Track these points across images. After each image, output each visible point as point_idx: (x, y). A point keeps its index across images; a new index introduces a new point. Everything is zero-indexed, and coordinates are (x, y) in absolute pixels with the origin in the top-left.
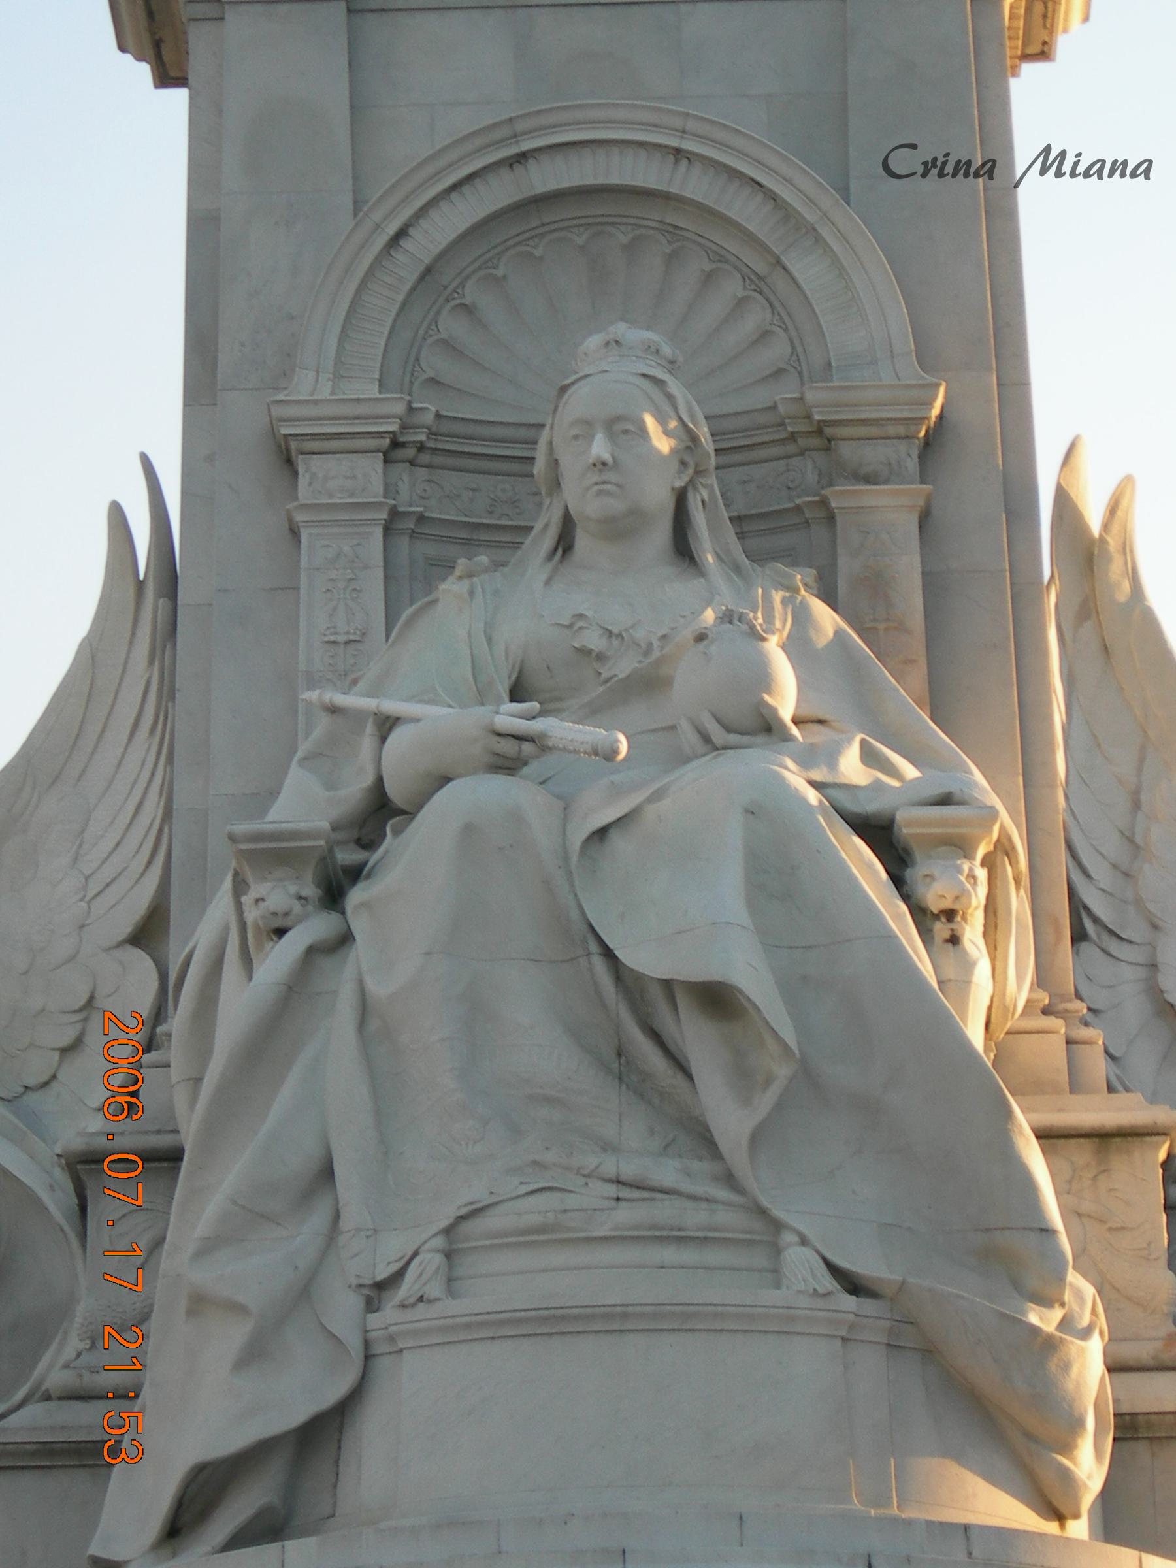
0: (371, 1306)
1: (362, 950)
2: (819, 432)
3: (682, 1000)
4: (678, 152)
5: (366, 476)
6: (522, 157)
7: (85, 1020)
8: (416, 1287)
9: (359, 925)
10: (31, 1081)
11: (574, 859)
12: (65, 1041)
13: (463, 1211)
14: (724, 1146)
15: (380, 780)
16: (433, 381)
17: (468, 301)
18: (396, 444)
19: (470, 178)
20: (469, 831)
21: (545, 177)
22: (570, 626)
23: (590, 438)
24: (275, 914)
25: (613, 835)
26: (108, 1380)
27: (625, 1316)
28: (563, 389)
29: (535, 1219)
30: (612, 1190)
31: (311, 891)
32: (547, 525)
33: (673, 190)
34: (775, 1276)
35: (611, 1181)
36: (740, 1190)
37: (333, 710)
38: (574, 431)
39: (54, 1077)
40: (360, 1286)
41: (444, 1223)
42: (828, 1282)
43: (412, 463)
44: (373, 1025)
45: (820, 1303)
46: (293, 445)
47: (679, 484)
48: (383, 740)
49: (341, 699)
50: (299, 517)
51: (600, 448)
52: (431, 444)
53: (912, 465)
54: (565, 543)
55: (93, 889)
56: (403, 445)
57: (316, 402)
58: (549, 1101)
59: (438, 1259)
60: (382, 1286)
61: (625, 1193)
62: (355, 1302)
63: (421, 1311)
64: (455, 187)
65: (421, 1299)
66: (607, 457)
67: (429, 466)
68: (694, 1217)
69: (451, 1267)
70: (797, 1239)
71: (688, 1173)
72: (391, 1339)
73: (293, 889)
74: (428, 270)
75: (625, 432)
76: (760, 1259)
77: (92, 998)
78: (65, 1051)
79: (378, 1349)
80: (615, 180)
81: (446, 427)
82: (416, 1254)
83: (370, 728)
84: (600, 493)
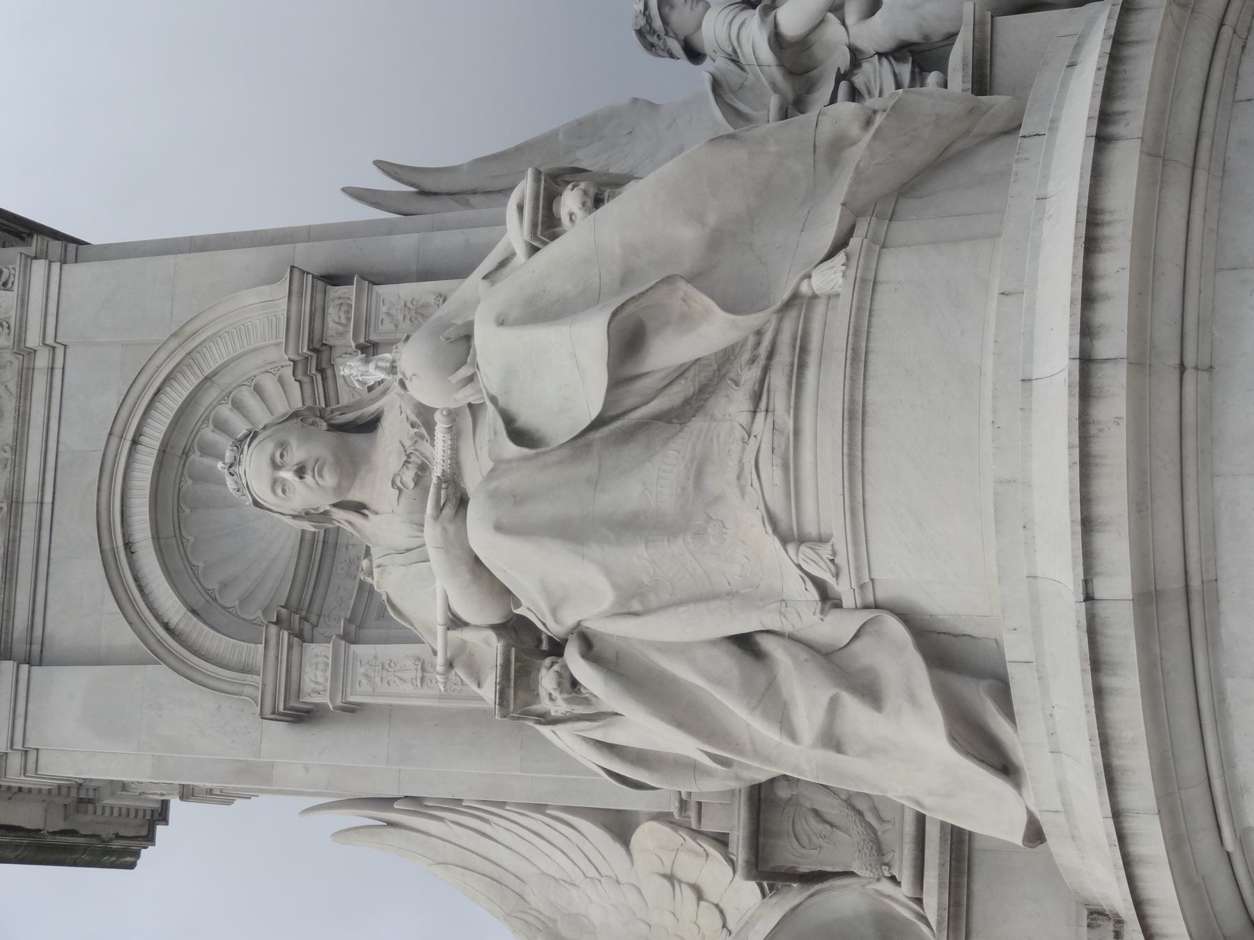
0: (838, 605)
4: (135, 442)
5: (318, 655)
6: (128, 545)
7: (680, 882)
8: (822, 564)
9: (569, 618)
10: (720, 923)
13: (769, 529)
15: (494, 627)
16: (265, 611)
17: (216, 587)
18: (300, 636)
19: (136, 579)
20: (499, 528)
22: (400, 490)
23: (284, 481)
24: (559, 684)
28: (256, 503)
29: (778, 474)
30: (760, 416)
31: (548, 661)
32: (350, 523)
33: (157, 445)
34: (833, 297)
35: (753, 418)
37: (450, 665)
38: (279, 491)
39: (717, 906)
40: (823, 612)
41: (778, 544)
42: (840, 257)
43: (314, 626)
44: (636, 606)
45: (854, 263)
46: (293, 704)
47: (324, 425)
48: (466, 624)
50: (339, 702)
52: (304, 613)
54: (359, 508)
55: (592, 872)
56: (301, 631)
57: (264, 685)
58: (699, 475)
59: (803, 548)
61: (763, 405)
62: (834, 615)
63: (841, 560)
67: (319, 616)
68: (784, 355)
69: (811, 540)
70: (806, 281)
71: (753, 361)
72: (862, 587)
73: (543, 672)
74: (194, 612)
75: (282, 456)
76: (820, 308)
77: (664, 876)
78: (700, 895)
79: (870, 599)
81: (294, 602)
82: (799, 567)
83: (456, 635)
84: (321, 475)
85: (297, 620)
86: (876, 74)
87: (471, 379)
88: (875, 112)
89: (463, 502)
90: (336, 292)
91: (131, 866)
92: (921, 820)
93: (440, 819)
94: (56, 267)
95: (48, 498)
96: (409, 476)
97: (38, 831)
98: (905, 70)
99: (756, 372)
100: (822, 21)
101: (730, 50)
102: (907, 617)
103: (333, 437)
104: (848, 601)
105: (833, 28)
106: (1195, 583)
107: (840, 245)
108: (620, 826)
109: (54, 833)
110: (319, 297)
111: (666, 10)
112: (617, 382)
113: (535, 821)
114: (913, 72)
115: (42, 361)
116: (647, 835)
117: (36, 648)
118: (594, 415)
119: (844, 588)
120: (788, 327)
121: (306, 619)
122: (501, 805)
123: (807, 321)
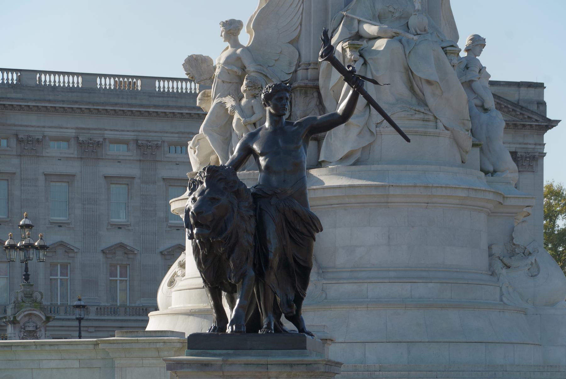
9: (369, 61)
10: (270, 65)
15: (358, 31)
30: (414, 112)
36: (431, 112)
42: (444, 129)
62: (375, 126)
68: (426, 117)
83: (356, 22)
99: (423, 111)
104: (378, 129)
106: (389, 204)
107: (447, 129)
108: (294, 42)
112: (420, 78)
116: (292, 48)
120: (432, 118)
122: (302, 14)
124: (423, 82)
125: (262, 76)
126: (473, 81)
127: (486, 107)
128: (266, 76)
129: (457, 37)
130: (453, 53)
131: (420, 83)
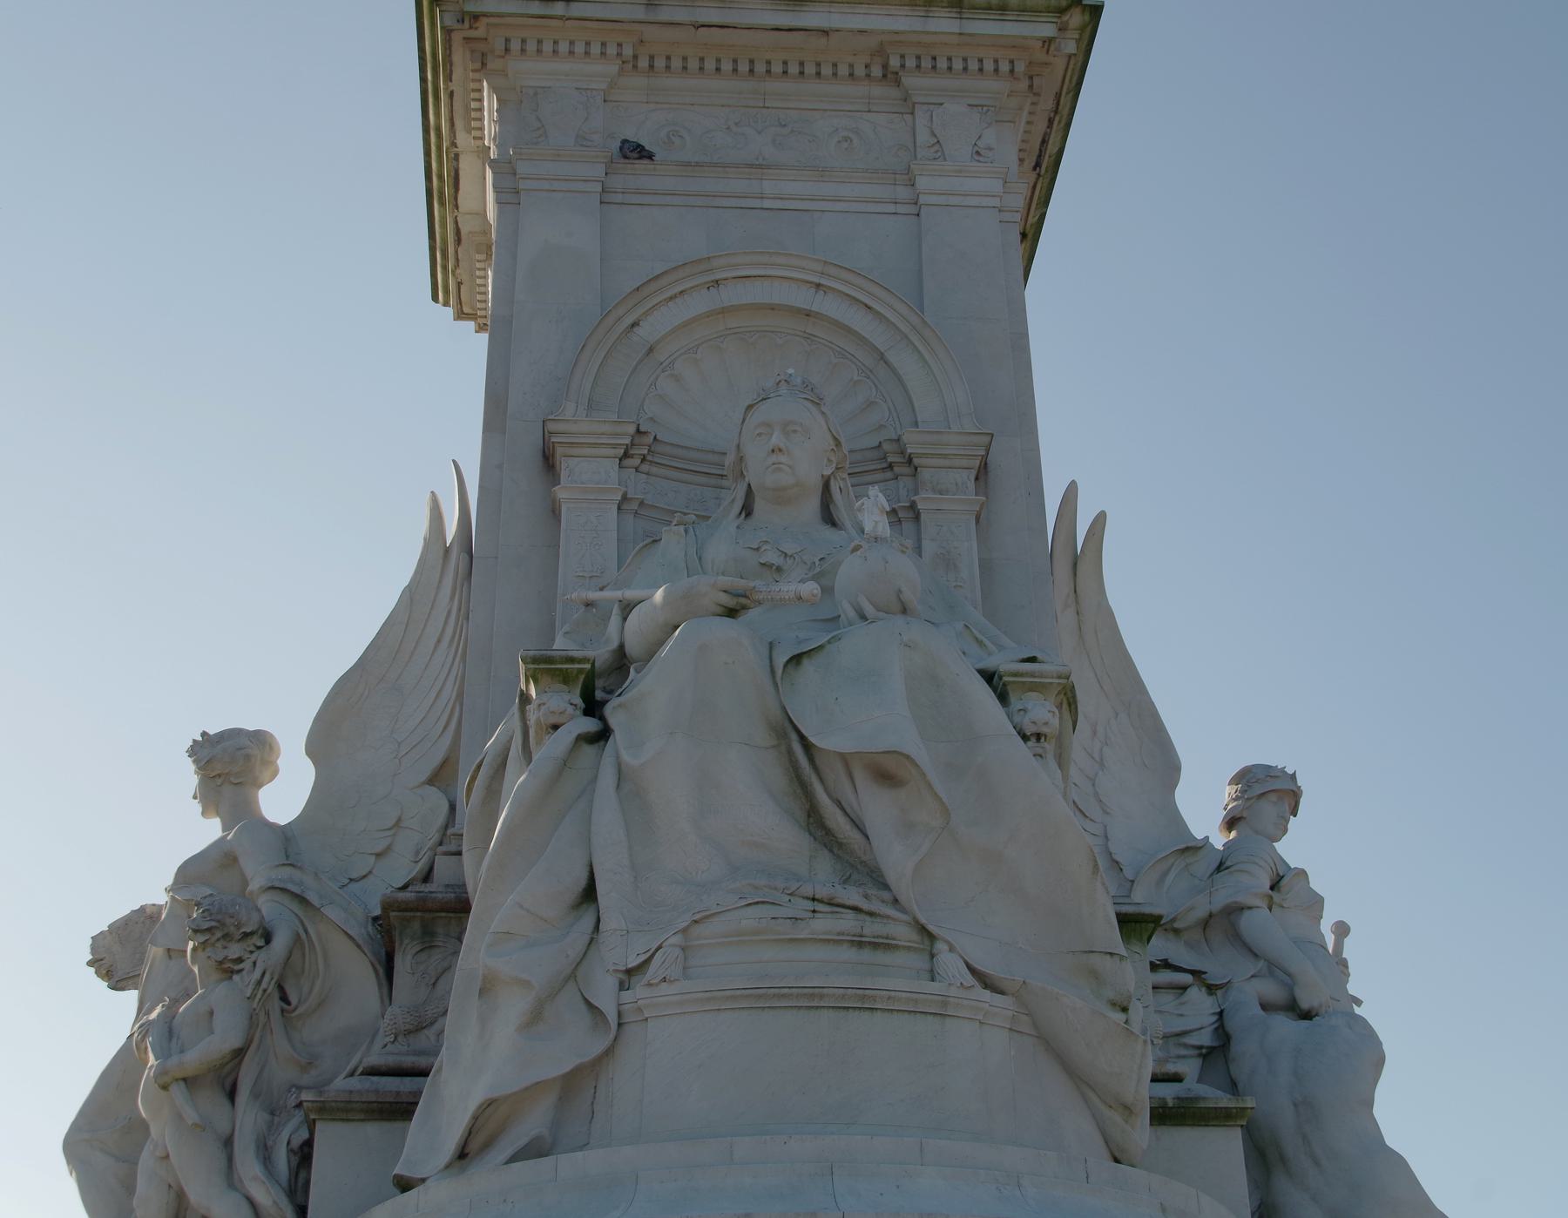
0: (623, 986)
1: (618, 737)
2: (910, 461)
3: (860, 776)
4: (818, 286)
10: (354, 876)
11: (779, 671)
12: (379, 849)
14: (891, 877)
15: (621, 647)
18: (626, 455)
21: (731, 295)
25: (805, 661)
26: (408, 1061)
27: (822, 997)
30: (810, 905)
36: (904, 911)
37: (589, 604)
40: (616, 971)
42: (969, 979)
46: (559, 451)
48: (625, 619)
49: (594, 595)
51: (776, 439)
53: (971, 485)
54: (747, 510)
56: (632, 456)
59: (677, 951)
60: (629, 972)
61: (820, 907)
62: (611, 982)
64: (671, 298)
65: (664, 980)
66: (782, 445)
68: (872, 929)
70: (946, 947)
71: (866, 896)
72: (640, 1010)
73: (567, 697)
74: (651, 350)
76: (918, 961)
77: (399, 820)
78: (378, 855)
80: (776, 300)
82: (660, 947)
83: (616, 610)
85: (640, 450)
86: (1198, 1010)
87: (863, 617)
88: (1125, 1010)
89: (732, 613)
90: (967, 478)
91: (435, 298)
92: (424, 1073)
93: (452, 598)
94: (995, 202)
95: (767, 204)
96: (771, 557)
97: (457, 207)
98: (1206, 1039)
100: (1256, 955)
101: (1228, 863)
102: (609, 1052)
103: (815, 482)
104: (627, 996)
105: (1252, 967)
109: (456, 222)
110: (964, 463)
111: (1273, 797)
113: (450, 691)
114: (1201, 1047)
115: (903, 193)
117: (619, 198)
118: (812, 739)
119: (639, 992)
120: (902, 932)
121: (644, 460)
123: (909, 948)
124: (860, 776)
125: (286, 900)
126: (1241, 909)
127: (1305, 1004)
128: (302, 900)
129: (1167, 767)
130: (1033, 688)
131: (848, 787)
